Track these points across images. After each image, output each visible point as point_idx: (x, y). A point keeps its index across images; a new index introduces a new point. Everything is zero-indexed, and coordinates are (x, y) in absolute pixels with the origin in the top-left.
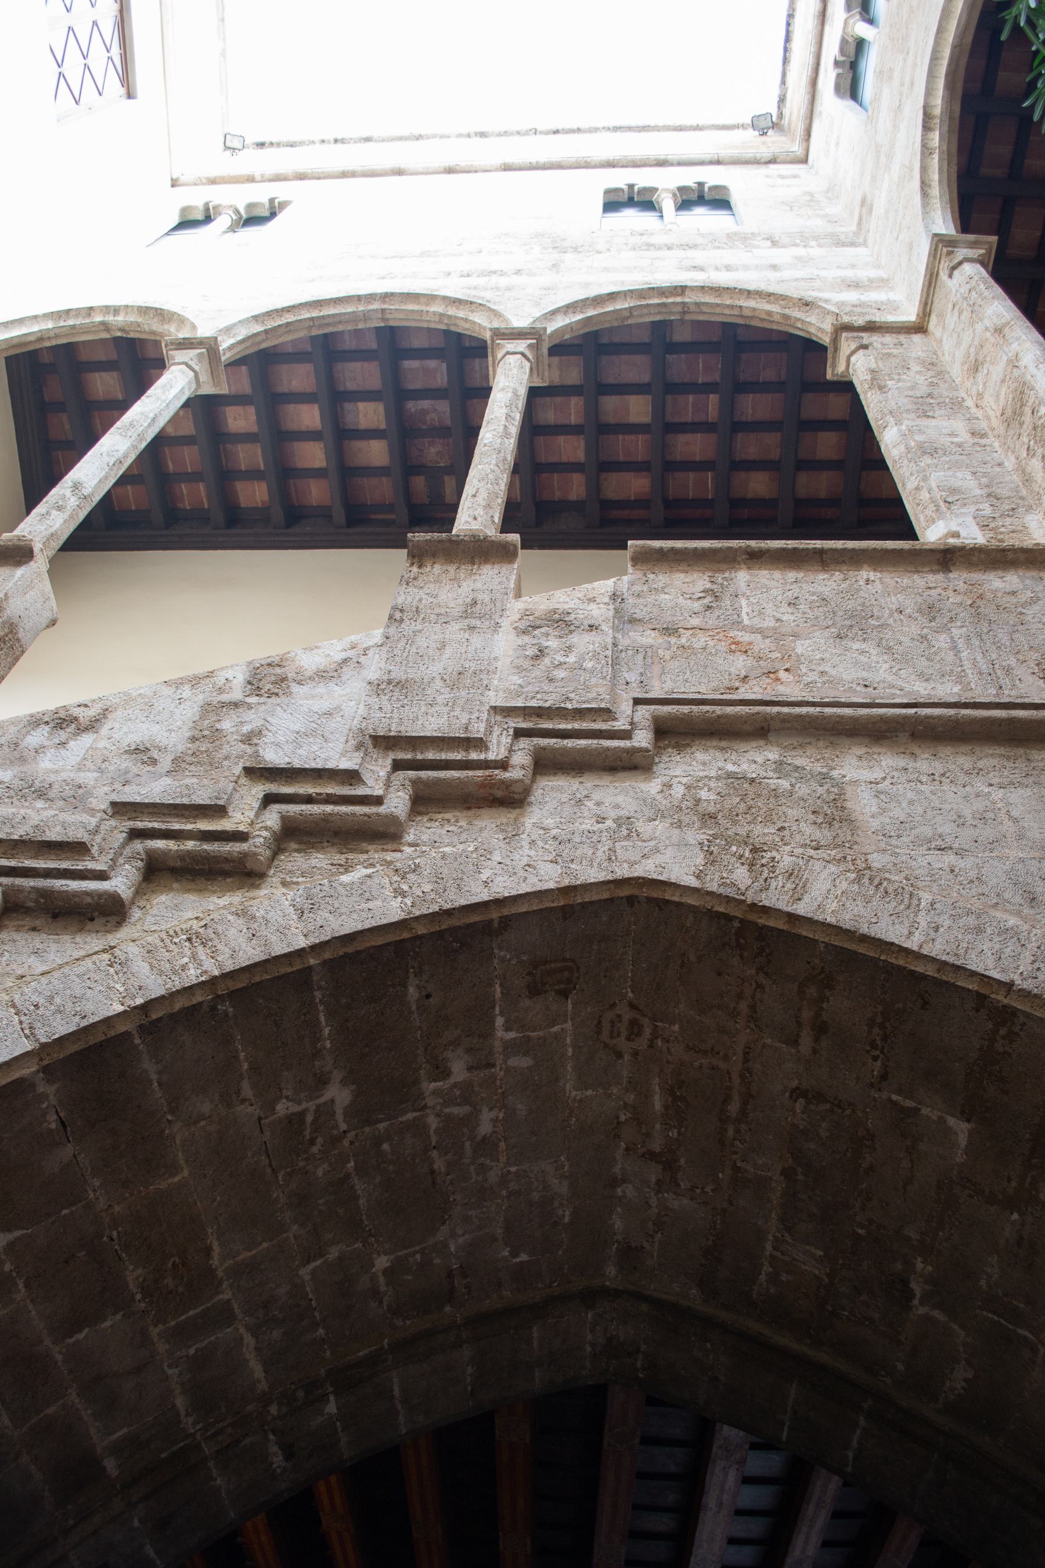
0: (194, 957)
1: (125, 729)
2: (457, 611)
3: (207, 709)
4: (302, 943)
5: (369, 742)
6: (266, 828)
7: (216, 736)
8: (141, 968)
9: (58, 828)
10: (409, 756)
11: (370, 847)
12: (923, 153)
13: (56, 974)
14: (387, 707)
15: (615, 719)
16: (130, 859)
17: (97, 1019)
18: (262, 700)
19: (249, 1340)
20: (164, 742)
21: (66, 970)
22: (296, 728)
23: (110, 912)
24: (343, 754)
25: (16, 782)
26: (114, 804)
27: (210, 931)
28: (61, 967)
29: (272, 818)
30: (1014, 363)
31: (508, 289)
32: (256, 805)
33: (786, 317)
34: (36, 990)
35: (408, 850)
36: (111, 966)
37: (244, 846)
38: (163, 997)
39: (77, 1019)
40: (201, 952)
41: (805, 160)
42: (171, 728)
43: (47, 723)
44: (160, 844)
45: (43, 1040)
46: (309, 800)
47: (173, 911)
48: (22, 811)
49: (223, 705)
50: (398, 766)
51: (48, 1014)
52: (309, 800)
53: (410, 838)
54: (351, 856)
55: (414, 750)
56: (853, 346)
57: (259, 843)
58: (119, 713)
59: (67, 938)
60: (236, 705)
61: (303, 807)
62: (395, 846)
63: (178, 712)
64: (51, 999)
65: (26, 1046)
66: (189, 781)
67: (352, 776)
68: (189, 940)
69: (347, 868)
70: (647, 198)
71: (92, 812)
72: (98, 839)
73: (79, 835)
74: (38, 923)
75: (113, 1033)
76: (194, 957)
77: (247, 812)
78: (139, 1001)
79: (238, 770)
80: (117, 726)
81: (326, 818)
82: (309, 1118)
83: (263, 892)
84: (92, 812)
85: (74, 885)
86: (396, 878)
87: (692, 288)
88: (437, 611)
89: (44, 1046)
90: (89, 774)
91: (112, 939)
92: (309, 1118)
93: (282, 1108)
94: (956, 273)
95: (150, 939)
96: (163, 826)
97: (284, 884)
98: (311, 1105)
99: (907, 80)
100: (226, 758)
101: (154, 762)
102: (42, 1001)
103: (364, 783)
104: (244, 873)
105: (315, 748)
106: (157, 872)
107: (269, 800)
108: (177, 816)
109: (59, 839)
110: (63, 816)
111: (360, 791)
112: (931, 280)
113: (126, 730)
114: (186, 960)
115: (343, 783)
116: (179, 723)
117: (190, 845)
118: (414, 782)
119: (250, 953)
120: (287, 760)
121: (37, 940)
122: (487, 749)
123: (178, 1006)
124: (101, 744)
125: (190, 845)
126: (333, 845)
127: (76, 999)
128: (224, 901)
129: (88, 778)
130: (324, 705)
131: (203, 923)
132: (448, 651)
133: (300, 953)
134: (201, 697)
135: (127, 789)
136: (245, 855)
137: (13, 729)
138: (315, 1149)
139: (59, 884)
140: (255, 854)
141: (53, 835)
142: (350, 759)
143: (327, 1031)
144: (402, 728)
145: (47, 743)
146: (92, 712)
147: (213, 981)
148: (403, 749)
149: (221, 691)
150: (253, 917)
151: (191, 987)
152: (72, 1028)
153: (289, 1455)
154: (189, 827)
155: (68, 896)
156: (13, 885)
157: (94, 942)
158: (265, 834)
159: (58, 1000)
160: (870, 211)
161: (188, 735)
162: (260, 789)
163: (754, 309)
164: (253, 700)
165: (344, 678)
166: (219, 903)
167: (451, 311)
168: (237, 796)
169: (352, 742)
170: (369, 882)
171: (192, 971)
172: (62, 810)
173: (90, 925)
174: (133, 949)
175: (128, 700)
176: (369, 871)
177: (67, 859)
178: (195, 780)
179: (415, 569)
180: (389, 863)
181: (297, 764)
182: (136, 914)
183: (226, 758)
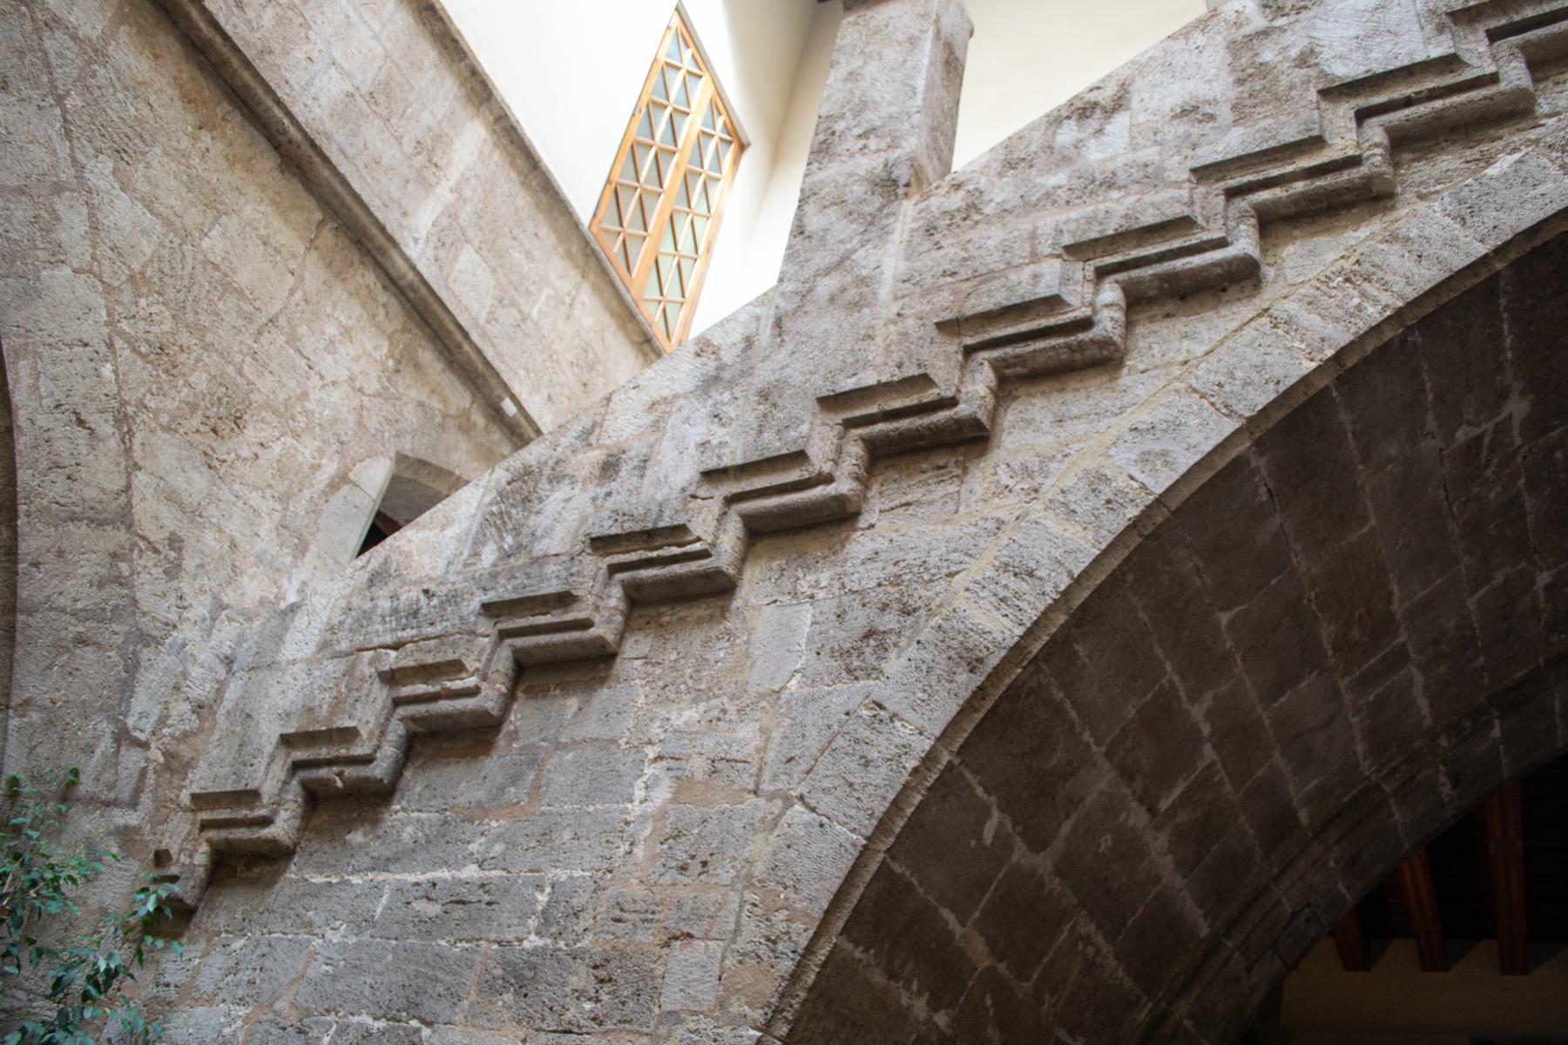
0: (1363, 295)
1: (1157, 96)
3: (1235, 48)
4: (1481, 250)
5: (1448, 21)
6: (1376, 145)
7: (1263, 70)
8: (1311, 320)
9: (1151, 211)
10: (1503, 21)
11: (1501, 132)
13: (1222, 350)
16: (1241, 218)
17: (1293, 381)
18: (1292, 18)
19: (1419, 678)
20: (1210, 95)
21: (1230, 343)
22: (1352, 32)
23: (1241, 278)
24: (1427, 41)
25: (1074, 181)
26: (1194, 171)
27: (1366, 265)
28: (1221, 343)
29: (1375, 132)
32: (1353, 125)
34: (1209, 371)
35: (1551, 121)
36: (1275, 326)
37: (1364, 170)
38: (1352, 343)
39: (1272, 386)
42: (1210, 77)
43: (1068, 117)
44: (1264, 195)
45: (1248, 414)
46: (1408, 102)
47: (1305, 261)
48: (1102, 206)
49: (1250, 38)
50: (1494, 36)
51: (1236, 389)
52: (1408, 102)
53: (1543, 106)
54: (1484, 147)
55: (1505, 13)
57: (1376, 160)
58: (1139, 83)
59: (1209, 314)
60: (1265, 33)
61: (1407, 111)
62: (1531, 123)
63: (1203, 60)
64: (1231, 374)
66: (1262, 124)
67: (1450, 62)
68: (1347, 280)
69: (1489, 161)
71: (1177, 184)
72: (1197, 208)
73: (1175, 211)
74: (1168, 309)
75: (1312, 391)
76: (1363, 295)
77: (1343, 134)
78: (1330, 353)
79: (1312, 95)
80: (1146, 96)
81: (1438, 116)
82: (1487, 440)
83: (1403, 212)
84: (1177, 184)
85: (1197, 260)
86: (1554, 155)
89: (1250, 420)
90: (1148, 151)
91: (1262, 301)
92: (1487, 440)
93: (1462, 435)
95: (1302, 291)
96: (1260, 177)
97: (1421, 197)
98: (1490, 426)
100: (1291, 88)
101: (1212, 117)
102: (1222, 379)
103: (1468, 65)
104: (1371, 198)
105: (1388, 46)
106: (1271, 223)
108: (1269, 162)
109: (1158, 220)
110: (1148, 198)
111: (1467, 75)
113: (1157, 99)
114: (1356, 301)
115: (1442, 73)
116: (1213, 71)
117: (1300, 186)
118: (1524, 48)
119: (1427, 276)
120: (1363, 68)
121: (1180, 324)
123: (1370, 348)
124: (1142, 118)
125: (1300, 186)
126: (1454, 142)
127: (1259, 368)
128: (1363, 232)
129: (1149, 154)
131: (1353, 260)
133: (1484, 261)
134: (1219, 38)
135: (1199, 151)
136: (1368, 180)
137: (1036, 135)
138: (1489, 472)
139: (1180, 264)
140: (1381, 175)
141: (1149, 218)
142: (1439, 44)
143: (1508, 341)
145: (1082, 136)
146: (1110, 91)
147: (1399, 314)
148: (1490, 17)
149: (1238, 25)
150: (1408, 239)
151: (1378, 325)
152: (1273, 396)
153: (1456, 781)
154: (1289, 169)
155: (1193, 274)
156: (1131, 279)
157: (1245, 310)
158: (1378, 151)
159: (1239, 374)
161: (1231, 79)
162: (1344, 112)
166: (1360, 237)
168: (1326, 122)
169: (1429, 28)
170: (1524, 167)
171: (1371, 310)
172: (1142, 193)
173: (1225, 296)
174: (1291, 306)
175: (1140, 67)
176: (1517, 156)
177: (1174, 238)
178: (1269, 121)
180: (1536, 142)
181: (1379, 68)
182: (1269, 272)
183: (1291, 88)
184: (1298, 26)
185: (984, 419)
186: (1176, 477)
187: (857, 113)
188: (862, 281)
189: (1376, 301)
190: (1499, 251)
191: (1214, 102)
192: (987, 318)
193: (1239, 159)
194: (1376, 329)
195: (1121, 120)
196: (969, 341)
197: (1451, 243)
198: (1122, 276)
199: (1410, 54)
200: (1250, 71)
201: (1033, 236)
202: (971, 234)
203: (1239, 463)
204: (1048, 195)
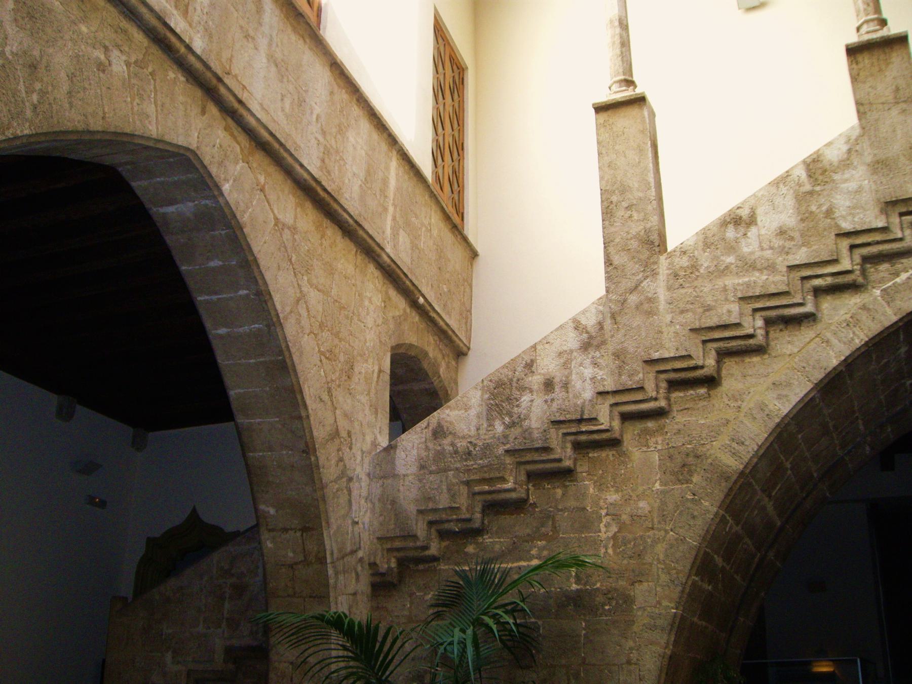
2: (891, 98)
9: (773, 286)
14: (884, 180)
22: (848, 203)
24: (876, 218)
26: (788, 267)
28: (803, 348)
29: (857, 259)
39: (822, 370)
40: (856, 330)
60: (811, 193)
64: (807, 363)
65: (810, 386)
66: (814, 247)
67: (884, 230)
76: (854, 333)
78: (843, 358)
79: (833, 237)
88: (880, 101)
100: (825, 229)
101: (792, 239)
105: (862, 216)
107: (853, 247)
113: (769, 222)
120: (852, 226)
127: (818, 361)
129: (768, 253)
130: (852, 185)
132: (899, 132)
133: (896, 322)
136: (855, 281)
144: (898, 195)
147: (867, 343)
162: (845, 243)
164: (818, 188)
165: (855, 163)
179: (854, 66)
183: (825, 229)
184: (825, 193)
185: (716, 375)
186: (791, 406)
187: (622, 193)
188: (650, 300)
189: (859, 337)
190: (901, 320)
191: (792, 229)
192: (711, 329)
194: (858, 349)
195: (753, 231)
196: (704, 338)
197: (884, 314)
198: (764, 313)
199: (870, 222)
200: (807, 215)
201: (725, 289)
202: (696, 283)
203: (812, 399)
204: (727, 267)
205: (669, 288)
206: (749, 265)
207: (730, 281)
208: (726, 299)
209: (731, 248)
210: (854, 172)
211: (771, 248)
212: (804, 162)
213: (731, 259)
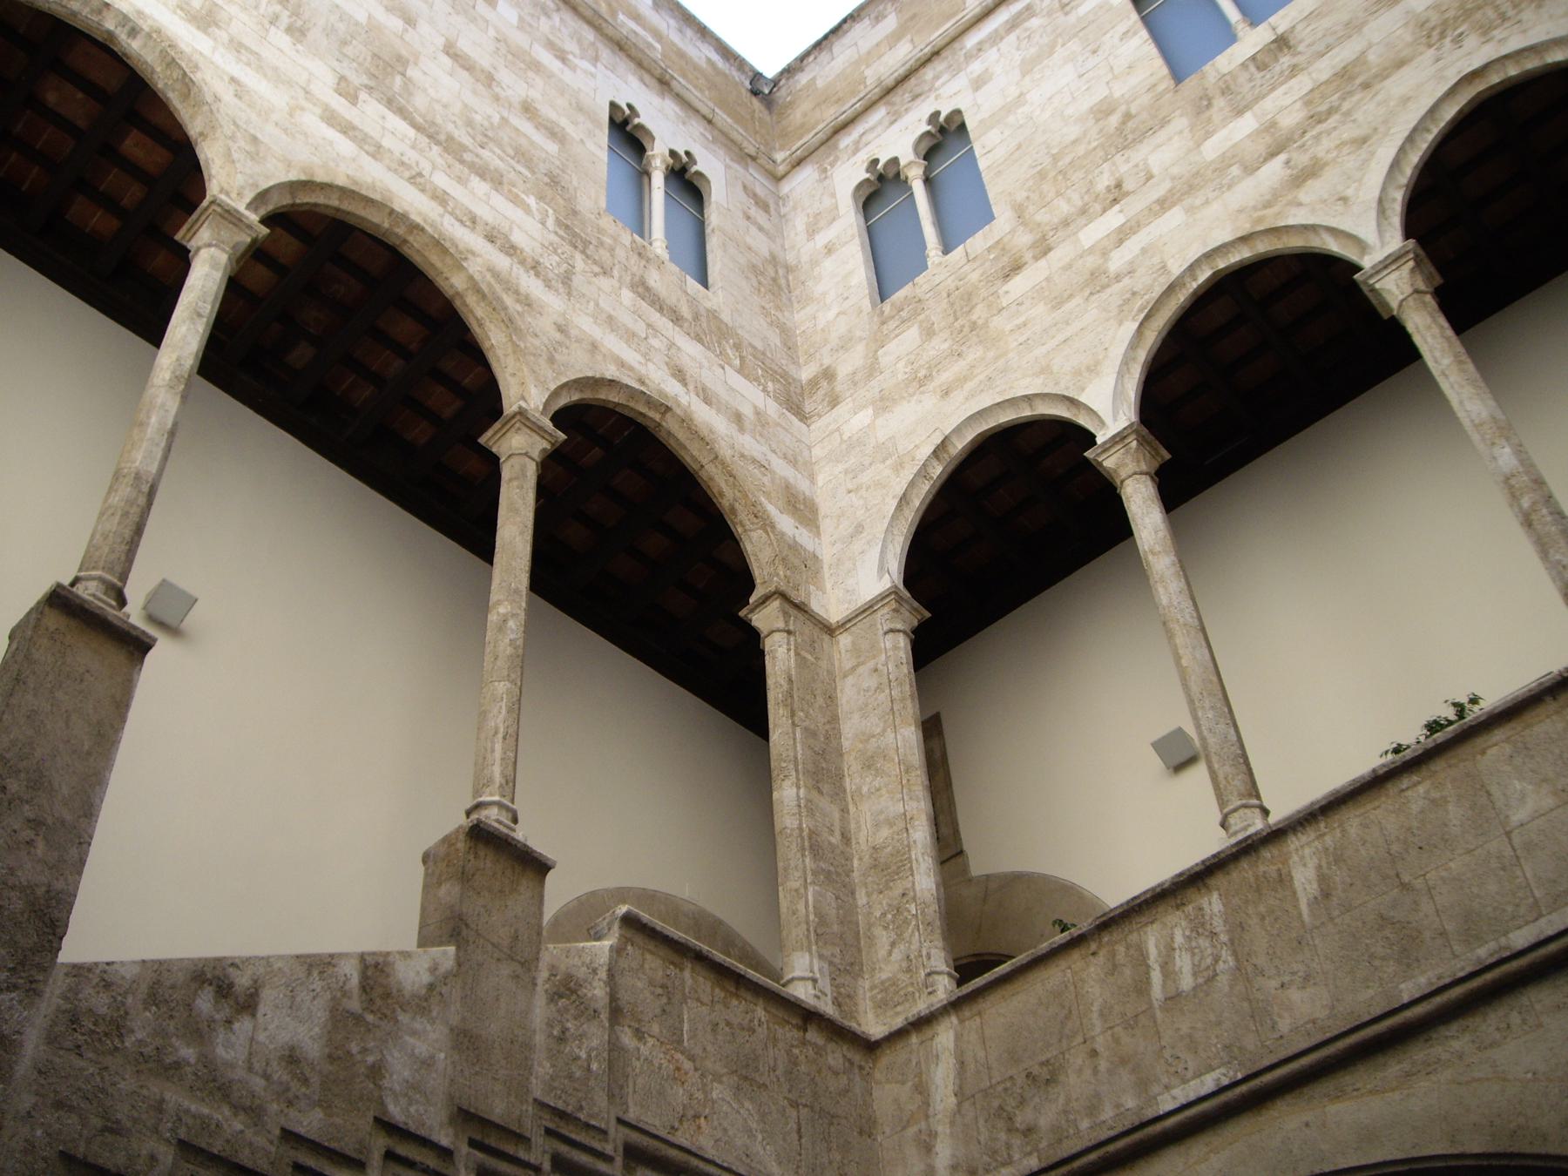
9: (247, 1151)
12: (919, 471)
15: (606, 1141)
26: (283, 1130)
30: (907, 819)
31: (528, 302)
33: (733, 510)
41: (778, 179)
56: (781, 625)
66: (338, 1121)
70: (638, 135)
87: (674, 415)
94: (891, 635)
99: (945, 377)
100: (361, 1098)
101: (305, 1081)
112: (869, 608)
122: (529, 1149)
129: (258, 1083)
160: (834, 402)
162: (381, 1142)
163: (711, 479)
164: (370, 1018)
165: (434, 1014)
167: (471, 300)
193: (312, 1142)
195: (243, 1025)
202: (107, 1060)
204: (177, 1065)
205: (52, 1039)
206: (215, 1084)
207: (176, 1097)
208: (156, 1130)
209: (198, 1032)
210: (429, 1028)
211: (266, 1077)
212: (362, 957)
213: (188, 1053)
